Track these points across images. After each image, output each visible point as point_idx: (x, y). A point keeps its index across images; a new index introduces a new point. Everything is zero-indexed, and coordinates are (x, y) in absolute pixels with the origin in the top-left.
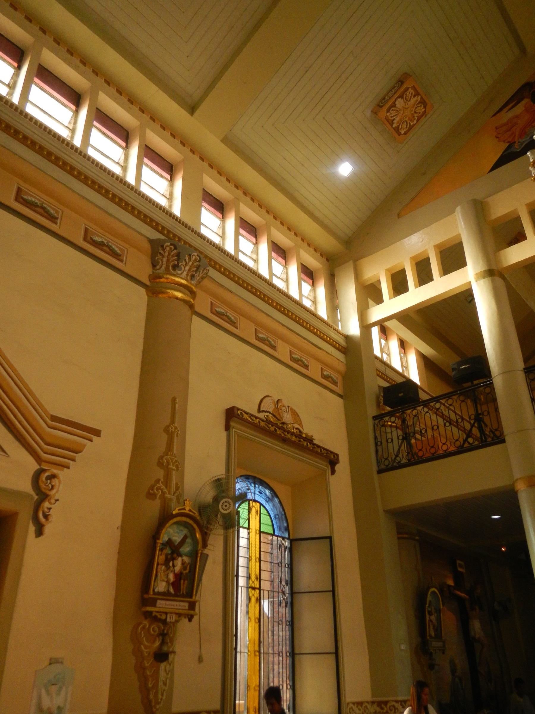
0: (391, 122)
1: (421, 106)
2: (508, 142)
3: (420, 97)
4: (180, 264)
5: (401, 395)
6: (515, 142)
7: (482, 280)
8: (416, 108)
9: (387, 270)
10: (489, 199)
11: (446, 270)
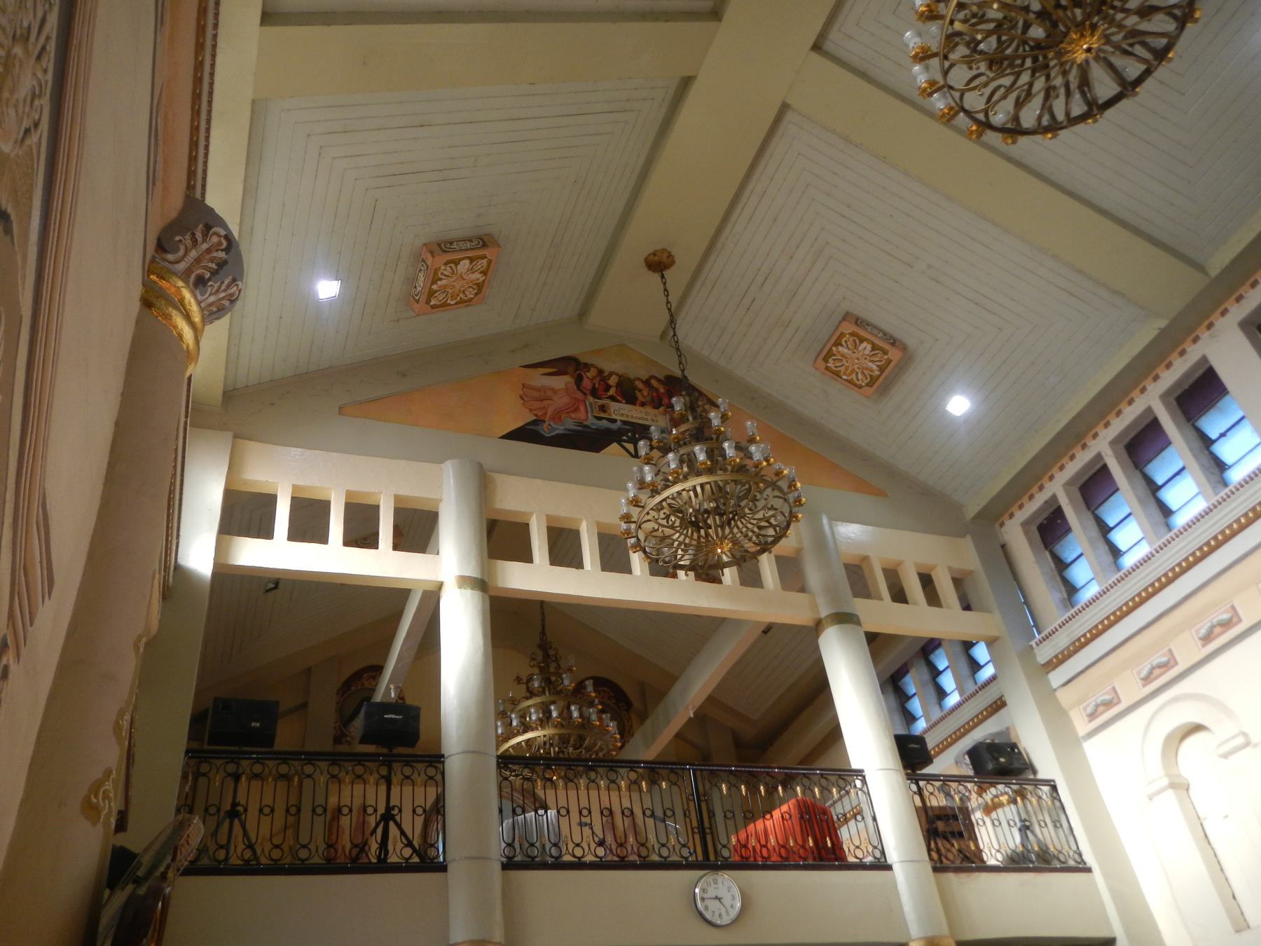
0: (436, 277)
1: (475, 289)
2: (536, 415)
3: (483, 278)
4: (210, 283)
5: (255, 724)
6: (544, 422)
7: (470, 591)
8: (470, 287)
9: (295, 488)
10: (498, 477)
11: (403, 542)
